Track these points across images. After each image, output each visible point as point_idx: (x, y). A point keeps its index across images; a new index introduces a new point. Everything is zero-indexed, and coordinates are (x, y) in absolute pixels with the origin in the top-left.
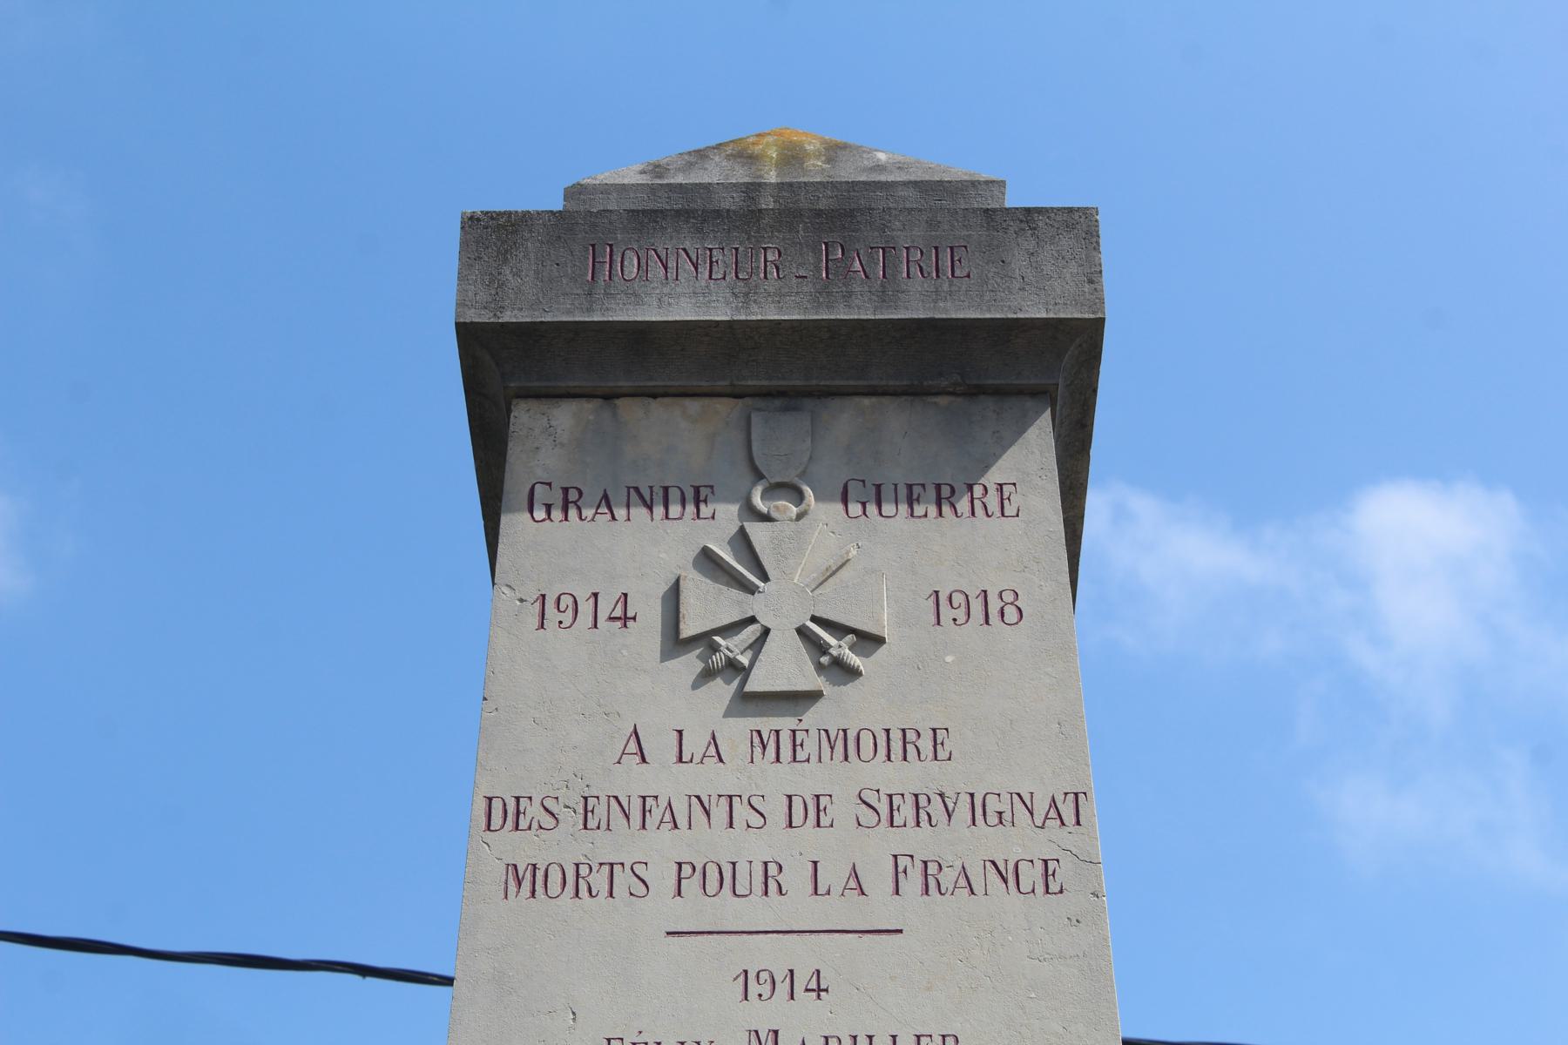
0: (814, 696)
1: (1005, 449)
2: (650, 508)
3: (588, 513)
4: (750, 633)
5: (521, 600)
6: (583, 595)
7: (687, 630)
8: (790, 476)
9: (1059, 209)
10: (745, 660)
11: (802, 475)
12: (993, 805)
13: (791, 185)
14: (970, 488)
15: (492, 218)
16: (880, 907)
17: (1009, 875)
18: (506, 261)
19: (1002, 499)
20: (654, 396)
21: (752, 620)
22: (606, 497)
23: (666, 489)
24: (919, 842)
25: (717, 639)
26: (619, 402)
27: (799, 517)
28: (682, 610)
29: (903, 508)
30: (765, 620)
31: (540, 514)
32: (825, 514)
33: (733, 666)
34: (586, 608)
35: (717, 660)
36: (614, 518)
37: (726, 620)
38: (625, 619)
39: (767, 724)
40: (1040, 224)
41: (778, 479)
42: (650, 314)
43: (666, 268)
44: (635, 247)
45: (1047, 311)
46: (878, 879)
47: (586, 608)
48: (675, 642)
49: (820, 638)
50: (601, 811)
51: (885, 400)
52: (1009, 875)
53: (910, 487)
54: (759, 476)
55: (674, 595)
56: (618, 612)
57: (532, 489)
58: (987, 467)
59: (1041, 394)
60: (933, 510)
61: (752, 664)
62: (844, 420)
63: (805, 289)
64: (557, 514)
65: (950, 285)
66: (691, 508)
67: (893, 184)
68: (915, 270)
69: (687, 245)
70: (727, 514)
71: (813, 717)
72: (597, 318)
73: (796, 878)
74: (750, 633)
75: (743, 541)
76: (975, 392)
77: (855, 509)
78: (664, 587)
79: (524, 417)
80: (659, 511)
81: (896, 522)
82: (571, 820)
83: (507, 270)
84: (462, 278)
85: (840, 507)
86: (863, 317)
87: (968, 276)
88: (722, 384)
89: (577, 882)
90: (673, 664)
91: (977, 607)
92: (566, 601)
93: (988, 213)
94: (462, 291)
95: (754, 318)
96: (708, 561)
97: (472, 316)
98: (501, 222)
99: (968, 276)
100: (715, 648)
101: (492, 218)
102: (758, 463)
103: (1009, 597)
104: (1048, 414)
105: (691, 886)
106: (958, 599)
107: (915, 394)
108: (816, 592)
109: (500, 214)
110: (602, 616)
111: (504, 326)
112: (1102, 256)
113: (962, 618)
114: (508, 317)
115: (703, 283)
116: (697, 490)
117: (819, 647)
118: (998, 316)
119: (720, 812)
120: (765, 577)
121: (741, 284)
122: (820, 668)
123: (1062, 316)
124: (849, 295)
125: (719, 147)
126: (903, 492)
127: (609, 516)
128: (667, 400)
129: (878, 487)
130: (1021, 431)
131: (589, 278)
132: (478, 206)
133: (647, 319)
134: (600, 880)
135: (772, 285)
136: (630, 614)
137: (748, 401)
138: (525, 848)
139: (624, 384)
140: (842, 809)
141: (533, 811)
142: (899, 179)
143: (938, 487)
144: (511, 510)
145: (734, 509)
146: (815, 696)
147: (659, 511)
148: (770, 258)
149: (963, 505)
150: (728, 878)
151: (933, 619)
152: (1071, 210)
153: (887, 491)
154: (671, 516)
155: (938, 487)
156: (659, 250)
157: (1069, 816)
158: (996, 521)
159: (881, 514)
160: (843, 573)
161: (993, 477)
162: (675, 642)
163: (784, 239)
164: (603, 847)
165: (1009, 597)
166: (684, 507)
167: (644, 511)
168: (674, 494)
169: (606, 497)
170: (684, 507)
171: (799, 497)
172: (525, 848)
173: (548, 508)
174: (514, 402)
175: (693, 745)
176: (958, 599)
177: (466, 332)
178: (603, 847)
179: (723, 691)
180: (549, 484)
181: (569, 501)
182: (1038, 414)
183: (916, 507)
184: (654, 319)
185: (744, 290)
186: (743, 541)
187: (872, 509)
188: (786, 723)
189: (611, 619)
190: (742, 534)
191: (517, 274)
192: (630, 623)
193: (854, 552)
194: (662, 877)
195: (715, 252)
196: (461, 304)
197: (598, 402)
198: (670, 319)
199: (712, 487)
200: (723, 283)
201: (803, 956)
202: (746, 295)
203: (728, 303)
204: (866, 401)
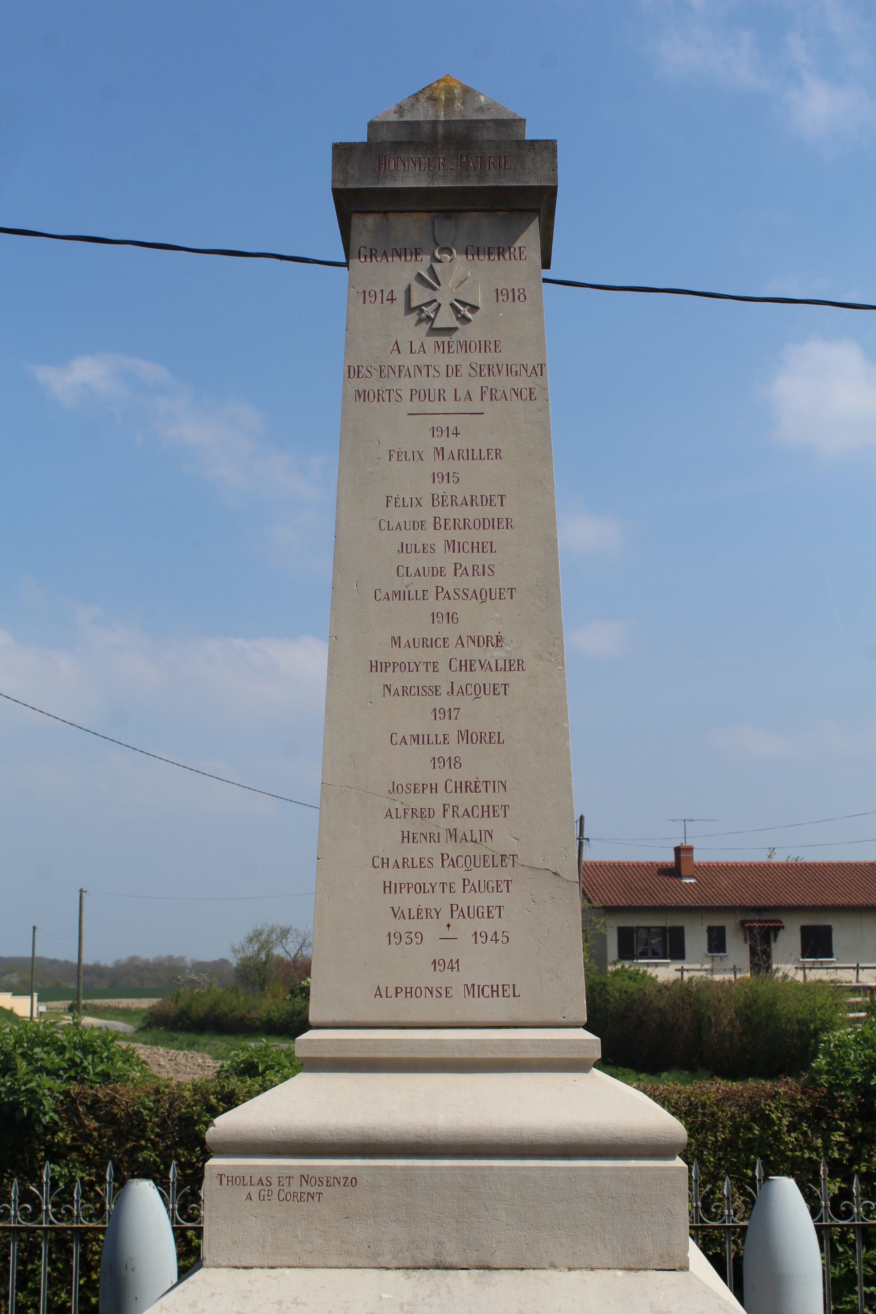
1: (522, 234)
2: (400, 257)
3: (379, 259)
4: (434, 305)
5: (357, 293)
6: (378, 291)
7: (414, 304)
8: (448, 245)
9: (543, 140)
10: (432, 316)
11: (452, 244)
13: (448, 121)
14: (510, 249)
15: (343, 145)
16: (476, 405)
18: (348, 163)
19: (520, 253)
21: (435, 301)
22: (385, 253)
23: (405, 250)
25: (423, 307)
26: (390, 215)
27: (451, 260)
28: (411, 297)
29: (487, 257)
30: (439, 301)
31: (363, 260)
32: (460, 259)
33: (428, 317)
34: (379, 295)
35: (423, 315)
36: (388, 261)
37: (426, 301)
38: (392, 300)
39: (440, 339)
40: (537, 147)
41: (443, 246)
43: (404, 165)
44: (393, 157)
45: (538, 183)
46: (476, 394)
47: (379, 295)
48: (409, 309)
49: (458, 307)
51: (481, 213)
53: (489, 248)
54: (437, 245)
55: (408, 291)
56: (390, 297)
57: (360, 250)
58: (515, 241)
59: (536, 211)
60: (496, 258)
61: (435, 317)
62: (467, 221)
63: (453, 174)
64: (368, 259)
65: (504, 172)
66: (414, 257)
67: (486, 121)
68: (491, 166)
69: (412, 156)
70: (427, 258)
71: (456, 337)
72: (380, 186)
73: (449, 395)
74: (434, 305)
75: (431, 270)
76: (512, 211)
77: (470, 257)
78: (405, 288)
79: (357, 221)
80: (403, 258)
81: (484, 263)
83: (349, 167)
84: (333, 170)
85: (465, 256)
86: (473, 185)
87: (510, 168)
88: (424, 208)
90: (409, 317)
91: (510, 295)
92: (372, 293)
93: (518, 141)
94: (333, 176)
95: (435, 186)
96: (420, 277)
98: (346, 146)
99: (510, 168)
100: (423, 311)
101: (343, 145)
102: (437, 240)
103: (521, 291)
104: (537, 219)
106: (504, 292)
107: (491, 211)
108: (457, 289)
109: (346, 143)
110: (385, 299)
112: (558, 160)
113: (505, 299)
115: (417, 172)
116: (416, 250)
117: (457, 311)
118: (520, 185)
120: (439, 284)
121: (431, 172)
123: (543, 185)
124: (468, 176)
125: (421, 92)
126: (486, 250)
127: (386, 260)
128: (405, 213)
129: (478, 248)
130: (527, 226)
131: (377, 170)
133: (398, 186)
135: (441, 173)
136: (394, 298)
137: (434, 214)
139: (390, 208)
142: (488, 118)
143: (499, 248)
144: (353, 258)
145: (429, 257)
147: (403, 258)
148: (441, 161)
149: (507, 256)
150: (427, 395)
151: (496, 300)
152: (547, 141)
153: (481, 250)
154: (407, 260)
155: (499, 248)
156: (402, 158)
158: (518, 262)
159: (479, 259)
160: (466, 282)
161: (518, 244)
163: (446, 153)
164: (388, 384)
165: (521, 291)
166: (411, 257)
167: (398, 258)
168: (408, 251)
169: (385, 253)
170: (411, 257)
171: (451, 253)
173: (366, 257)
174: (353, 214)
176: (504, 292)
177: (335, 192)
178: (388, 384)
179: (425, 327)
180: (365, 247)
181: (372, 255)
182: (534, 219)
183: (491, 257)
184: (400, 186)
185: (432, 174)
186: (431, 270)
187: (476, 257)
188: (446, 339)
189: (388, 300)
190: (431, 267)
191: (352, 168)
192: (394, 301)
193: (469, 274)
195: (421, 159)
196: (333, 181)
197: (382, 214)
198: (406, 186)
199: (421, 249)
200: (425, 172)
201: (452, 422)
202: (433, 176)
203: (426, 180)
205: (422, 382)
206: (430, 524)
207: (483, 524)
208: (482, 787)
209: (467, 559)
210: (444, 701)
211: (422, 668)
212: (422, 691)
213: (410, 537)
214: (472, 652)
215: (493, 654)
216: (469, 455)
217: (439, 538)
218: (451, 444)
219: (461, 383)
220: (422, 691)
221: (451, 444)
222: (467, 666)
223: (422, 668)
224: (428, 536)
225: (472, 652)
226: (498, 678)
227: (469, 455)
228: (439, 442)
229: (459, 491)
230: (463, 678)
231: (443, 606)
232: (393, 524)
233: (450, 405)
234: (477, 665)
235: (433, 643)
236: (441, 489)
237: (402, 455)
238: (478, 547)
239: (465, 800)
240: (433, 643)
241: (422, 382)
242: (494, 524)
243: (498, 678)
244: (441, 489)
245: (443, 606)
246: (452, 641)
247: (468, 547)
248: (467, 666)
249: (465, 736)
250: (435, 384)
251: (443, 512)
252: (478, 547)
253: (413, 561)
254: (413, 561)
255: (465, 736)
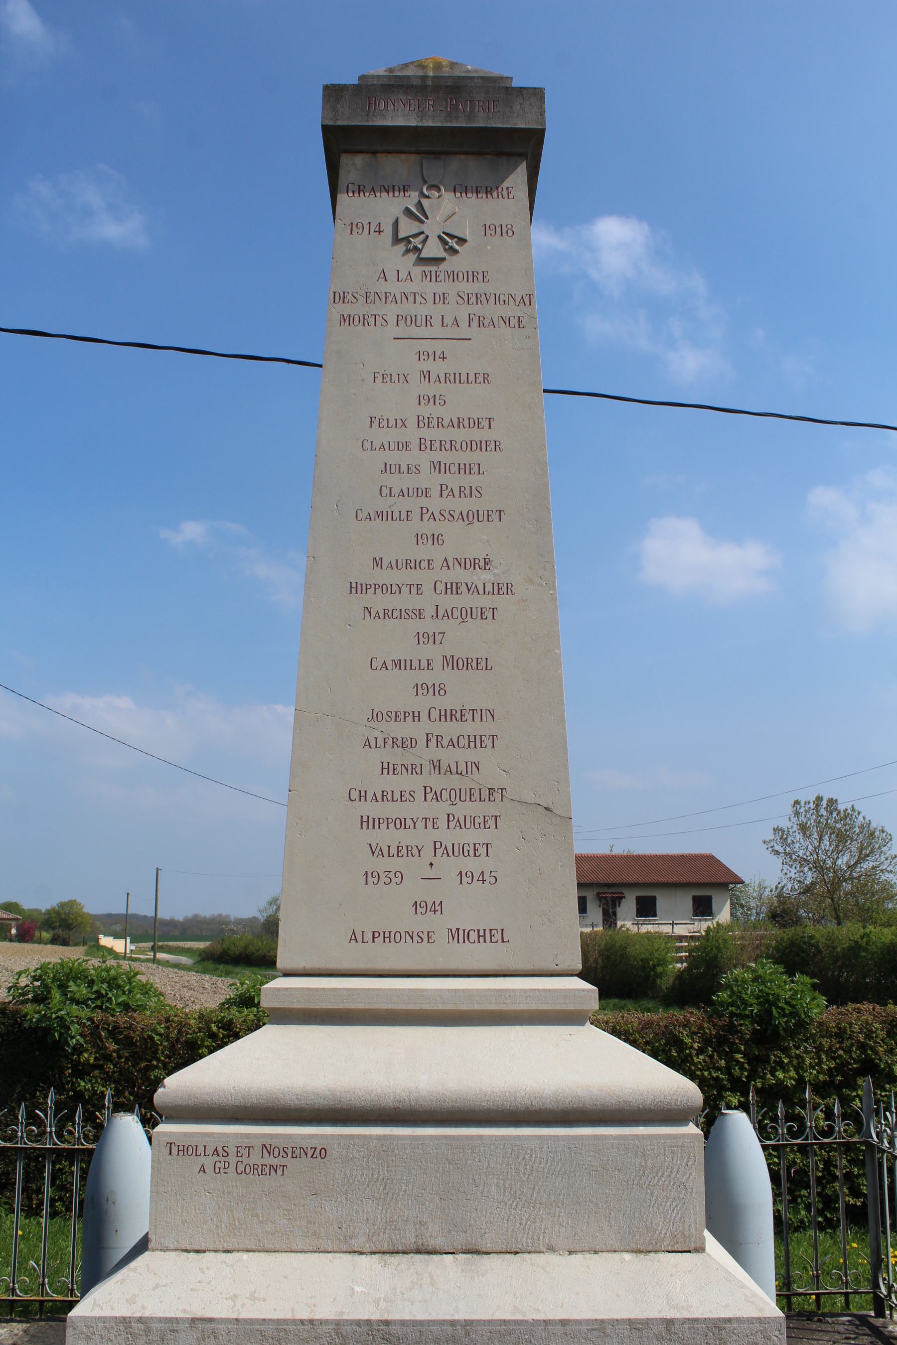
0: (443, 259)
2: (388, 193)
4: (422, 237)
7: (401, 235)
9: (531, 88)
10: (420, 247)
11: (440, 182)
12: (502, 298)
13: (437, 76)
16: (464, 331)
17: (506, 321)
18: (338, 102)
20: (390, 153)
21: (423, 233)
23: (394, 186)
24: (477, 309)
25: (411, 239)
26: (379, 155)
28: (399, 229)
29: (475, 195)
30: (426, 233)
31: (351, 194)
33: (416, 249)
34: (366, 227)
35: (411, 246)
36: (376, 196)
38: (380, 232)
39: (427, 269)
41: (432, 183)
42: (389, 123)
43: (394, 106)
46: (464, 322)
47: (366, 227)
48: (396, 240)
50: (372, 297)
52: (506, 321)
53: (477, 188)
54: (425, 182)
55: (396, 224)
56: (377, 229)
58: (503, 181)
59: (522, 155)
60: (484, 196)
61: (422, 248)
62: (455, 163)
64: (356, 194)
66: (402, 193)
69: (402, 98)
70: (414, 195)
71: (443, 267)
72: (370, 124)
73: (436, 321)
74: (422, 237)
75: (420, 205)
76: (500, 154)
78: (392, 221)
79: (345, 160)
80: (391, 194)
81: (472, 200)
82: (362, 300)
84: (323, 108)
85: (453, 194)
89: (364, 321)
91: (498, 230)
93: (507, 88)
94: (323, 113)
95: (424, 125)
96: (408, 212)
97: (327, 122)
98: (337, 87)
100: (410, 242)
103: (509, 227)
104: (525, 162)
105: (402, 323)
106: (492, 227)
107: (480, 154)
108: (445, 223)
110: (372, 230)
111: (339, 126)
113: (493, 234)
114: (339, 123)
116: (404, 187)
117: (444, 243)
118: (509, 126)
119: (411, 298)
120: (427, 218)
121: (420, 112)
122: (445, 250)
123: (531, 127)
124: (458, 117)
125: (412, 62)
126: (474, 189)
128: (394, 154)
129: (466, 187)
132: (329, 82)
134: (371, 320)
137: (422, 155)
138: (347, 309)
140: (452, 298)
141: (349, 297)
143: (487, 188)
144: (341, 193)
145: (417, 194)
146: (443, 259)
147: (391, 194)
148: (430, 103)
149: (495, 195)
150: (414, 320)
151: (484, 234)
152: (535, 88)
153: (469, 189)
155: (487, 188)
157: (527, 302)
158: (506, 201)
160: (454, 217)
161: (506, 184)
162: (396, 240)
164: (373, 309)
165: (509, 227)
167: (386, 194)
168: (396, 188)
169: (373, 189)
171: (439, 190)
172: (347, 309)
174: (342, 154)
175: (403, 275)
176: (492, 227)
177: (326, 129)
178: (373, 309)
179: (412, 257)
180: (354, 184)
182: (521, 163)
184: (390, 125)
186: (420, 205)
187: (464, 195)
188: (433, 269)
189: (375, 231)
190: (419, 202)
191: (342, 107)
192: (381, 233)
194: (392, 320)
196: (323, 118)
197: (371, 154)
198: (396, 124)
199: (409, 186)
201: (439, 347)
202: (422, 116)
203: (415, 120)
204: (463, 157)
205: (409, 308)
206: (414, 445)
207: (469, 445)
208: (468, 716)
209: (454, 481)
210: (428, 625)
211: (405, 590)
212: (404, 614)
213: (394, 457)
214: (457, 575)
215: (481, 577)
216: (456, 378)
217: (424, 459)
218: (438, 368)
219: (449, 310)
220: (404, 614)
221: (438, 368)
222: (453, 588)
223: (405, 590)
224: (413, 456)
225: (457, 575)
226: (486, 601)
227: (456, 378)
228: (426, 365)
229: (446, 413)
230: (448, 601)
231: (428, 527)
232: (377, 445)
233: (436, 330)
234: (463, 588)
235: (417, 565)
236: (426, 410)
237: (386, 378)
238: (465, 469)
239: (451, 729)
240: (417, 565)
241: (409, 308)
242: (482, 446)
243: (486, 601)
244: (426, 410)
245: (428, 527)
246: (438, 563)
247: (454, 469)
248: (453, 588)
249: (451, 662)
250: (422, 311)
251: (428, 434)
252: (465, 469)
253: (396, 482)
254: (396, 482)
255: (451, 662)
